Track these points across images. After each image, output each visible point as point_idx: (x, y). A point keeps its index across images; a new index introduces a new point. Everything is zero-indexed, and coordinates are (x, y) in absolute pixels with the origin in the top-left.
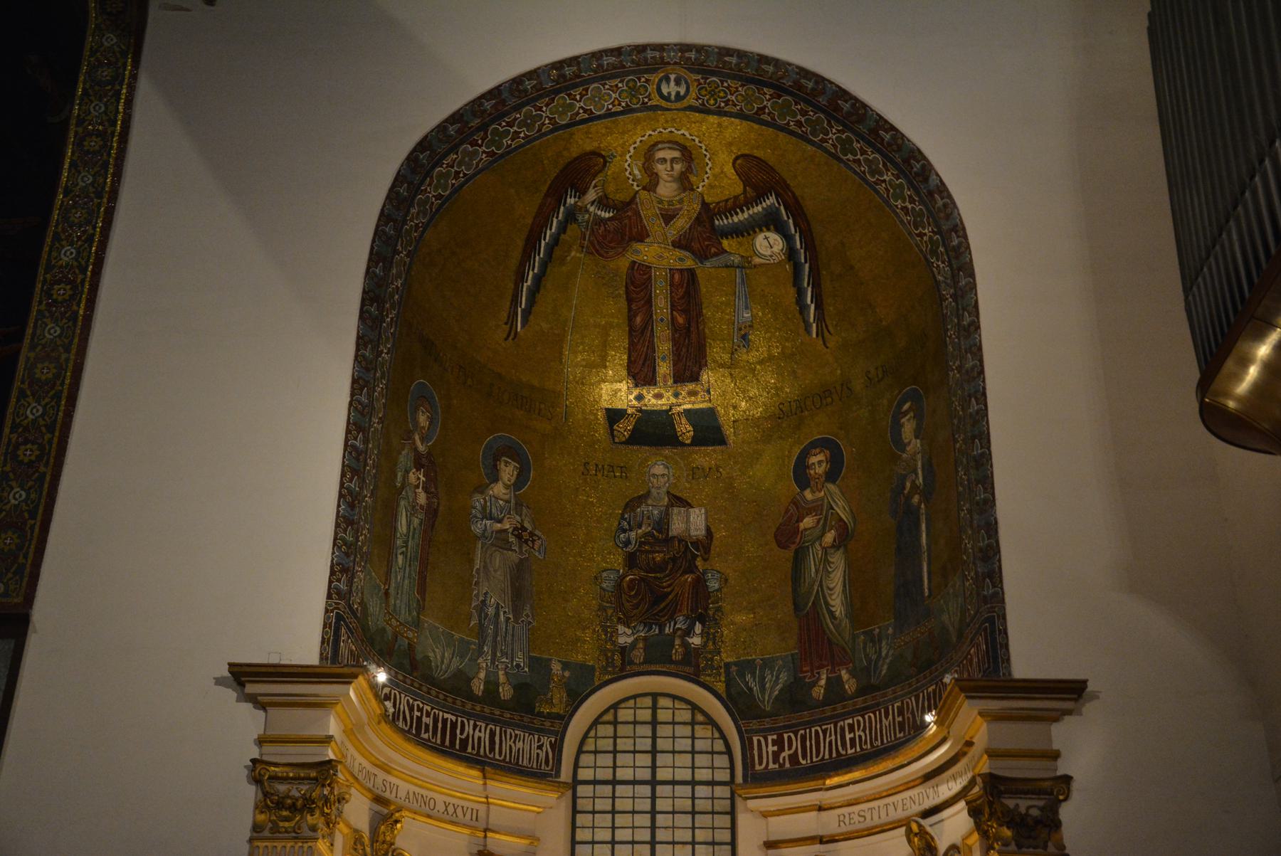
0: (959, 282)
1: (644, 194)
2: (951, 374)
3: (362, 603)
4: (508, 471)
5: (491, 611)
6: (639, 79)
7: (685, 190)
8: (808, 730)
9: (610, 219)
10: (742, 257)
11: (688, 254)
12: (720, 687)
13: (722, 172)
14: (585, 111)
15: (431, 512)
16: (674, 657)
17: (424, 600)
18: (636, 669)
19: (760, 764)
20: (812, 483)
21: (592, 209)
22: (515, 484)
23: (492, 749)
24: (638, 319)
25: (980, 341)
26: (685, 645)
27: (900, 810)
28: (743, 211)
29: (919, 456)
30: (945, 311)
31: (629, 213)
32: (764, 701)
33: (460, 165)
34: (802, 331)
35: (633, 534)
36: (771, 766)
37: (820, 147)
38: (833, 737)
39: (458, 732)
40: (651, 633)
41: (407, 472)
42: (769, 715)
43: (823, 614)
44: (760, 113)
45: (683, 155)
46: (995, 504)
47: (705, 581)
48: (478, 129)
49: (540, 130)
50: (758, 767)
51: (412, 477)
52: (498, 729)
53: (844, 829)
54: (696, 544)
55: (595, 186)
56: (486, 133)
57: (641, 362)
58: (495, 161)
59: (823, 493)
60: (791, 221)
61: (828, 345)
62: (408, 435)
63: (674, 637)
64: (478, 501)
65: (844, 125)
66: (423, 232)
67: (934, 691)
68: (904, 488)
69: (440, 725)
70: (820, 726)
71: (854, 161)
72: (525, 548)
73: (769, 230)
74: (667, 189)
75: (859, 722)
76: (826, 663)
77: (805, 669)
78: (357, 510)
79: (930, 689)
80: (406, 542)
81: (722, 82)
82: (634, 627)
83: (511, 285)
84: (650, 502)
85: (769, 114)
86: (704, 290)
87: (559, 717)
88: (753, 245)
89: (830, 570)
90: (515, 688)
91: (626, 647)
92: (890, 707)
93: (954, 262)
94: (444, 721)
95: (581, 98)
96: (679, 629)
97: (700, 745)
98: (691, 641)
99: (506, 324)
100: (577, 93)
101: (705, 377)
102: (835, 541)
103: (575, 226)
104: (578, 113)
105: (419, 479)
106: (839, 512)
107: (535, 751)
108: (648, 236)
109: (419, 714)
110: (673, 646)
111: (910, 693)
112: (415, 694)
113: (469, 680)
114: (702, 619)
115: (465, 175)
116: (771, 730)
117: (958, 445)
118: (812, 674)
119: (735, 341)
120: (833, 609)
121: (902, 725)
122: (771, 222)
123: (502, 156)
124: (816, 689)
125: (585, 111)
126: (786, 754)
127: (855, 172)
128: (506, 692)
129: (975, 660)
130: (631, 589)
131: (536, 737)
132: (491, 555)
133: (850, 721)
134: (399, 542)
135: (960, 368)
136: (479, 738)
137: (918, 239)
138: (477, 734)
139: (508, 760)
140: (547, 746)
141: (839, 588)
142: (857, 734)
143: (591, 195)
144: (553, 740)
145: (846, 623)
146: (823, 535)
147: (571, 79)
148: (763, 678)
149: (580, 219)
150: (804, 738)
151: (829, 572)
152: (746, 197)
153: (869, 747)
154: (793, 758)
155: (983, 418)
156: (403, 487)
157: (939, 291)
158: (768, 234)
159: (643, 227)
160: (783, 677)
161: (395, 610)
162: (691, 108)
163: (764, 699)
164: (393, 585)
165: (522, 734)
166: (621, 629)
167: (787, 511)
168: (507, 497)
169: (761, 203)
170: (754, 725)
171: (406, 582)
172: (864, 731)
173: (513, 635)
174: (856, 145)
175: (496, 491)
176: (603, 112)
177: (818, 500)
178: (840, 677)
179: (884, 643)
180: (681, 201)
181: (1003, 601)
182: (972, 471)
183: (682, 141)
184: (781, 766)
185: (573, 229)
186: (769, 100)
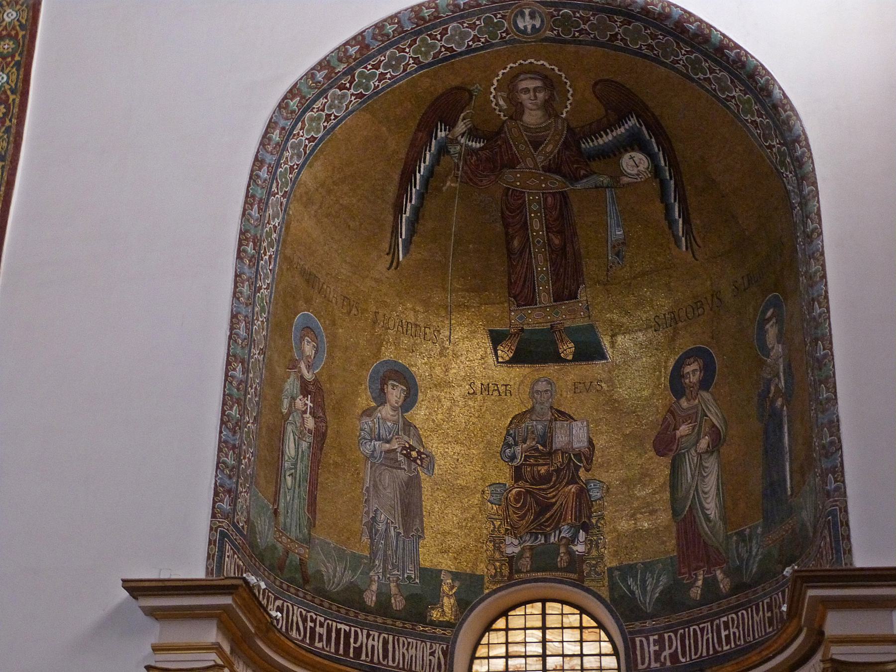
3: (248, 521)
6: (495, 16)
12: (605, 593)
15: (320, 436)
16: (559, 564)
23: (385, 656)
25: (823, 247)
26: (570, 553)
28: (607, 134)
32: (645, 603)
39: (352, 640)
42: (651, 617)
43: (699, 517)
47: (588, 491)
51: (299, 403)
52: (391, 638)
54: (578, 456)
60: (653, 140)
63: (559, 546)
69: (334, 635)
73: (633, 150)
74: (532, 117)
77: (683, 571)
80: (295, 465)
81: (574, 13)
82: (521, 538)
88: (619, 165)
89: (705, 474)
91: (513, 556)
94: (338, 631)
95: (441, 38)
98: (575, 548)
102: (708, 446)
105: (306, 404)
106: (712, 418)
107: (427, 658)
110: (559, 554)
112: (307, 605)
113: (361, 592)
114: (586, 527)
118: (690, 574)
120: (708, 512)
122: (634, 142)
132: (381, 474)
136: (373, 646)
139: (401, 666)
141: (713, 492)
146: (697, 441)
147: (430, 20)
148: (644, 581)
151: (704, 477)
155: (825, 320)
156: (290, 413)
158: (633, 154)
160: (664, 580)
163: (645, 601)
166: (509, 539)
170: (638, 625)
173: (404, 549)
177: (692, 408)
178: (715, 577)
179: (754, 542)
181: (845, 494)
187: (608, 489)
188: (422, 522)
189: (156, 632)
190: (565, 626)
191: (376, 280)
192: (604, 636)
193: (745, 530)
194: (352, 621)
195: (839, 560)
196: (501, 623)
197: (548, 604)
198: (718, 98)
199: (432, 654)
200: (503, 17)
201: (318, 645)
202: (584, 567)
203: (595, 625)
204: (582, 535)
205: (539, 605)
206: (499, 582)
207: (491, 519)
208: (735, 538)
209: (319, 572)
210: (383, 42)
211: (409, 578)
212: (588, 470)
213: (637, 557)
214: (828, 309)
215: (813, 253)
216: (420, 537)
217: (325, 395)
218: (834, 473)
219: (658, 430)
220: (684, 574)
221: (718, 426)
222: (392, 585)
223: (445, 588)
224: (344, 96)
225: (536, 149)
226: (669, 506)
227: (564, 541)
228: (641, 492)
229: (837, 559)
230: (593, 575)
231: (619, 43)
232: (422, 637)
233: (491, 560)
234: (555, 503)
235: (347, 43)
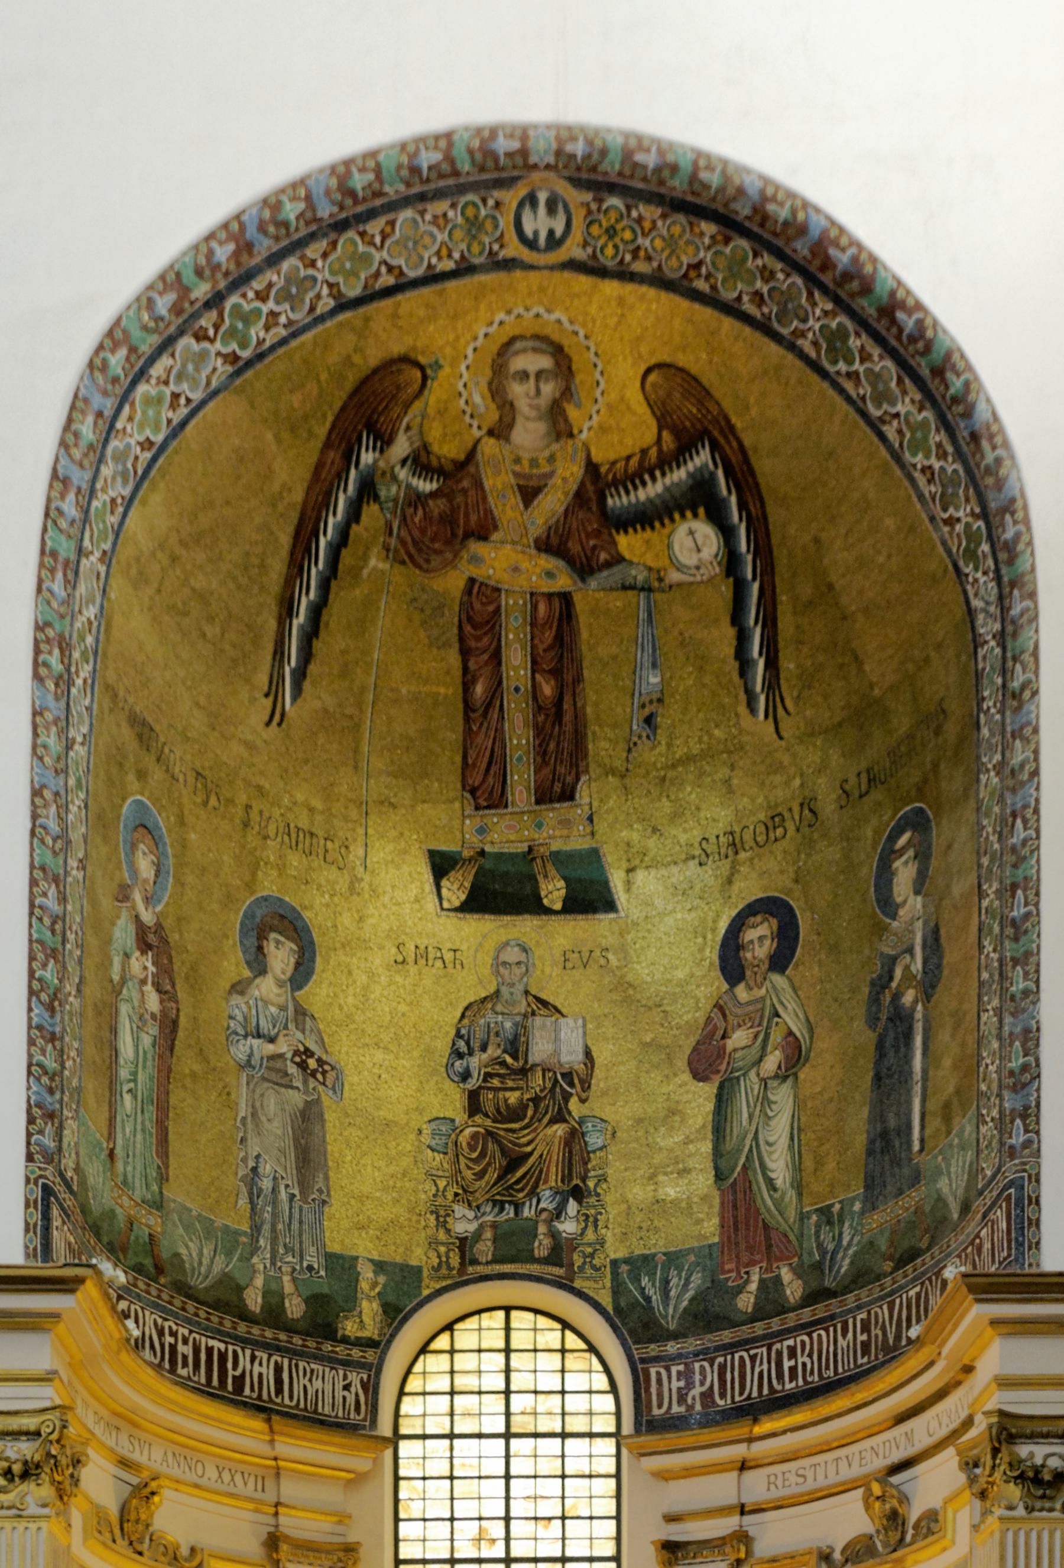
0: (1009, 608)
1: (490, 447)
2: (983, 778)
6: (484, 201)
7: (558, 437)
8: (729, 1357)
10: (650, 569)
11: (561, 564)
12: (606, 1299)
13: (622, 399)
14: (390, 269)
16: (536, 1252)
17: (167, 1167)
18: (481, 1269)
19: (660, 1406)
20: (748, 973)
22: (291, 980)
26: (554, 1235)
27: (855, 1464)
29: (919, 924)
30: (980, 666)
32: (666, 1316)
33: (180, 377)
34: (742, 709)
35: (474, 1062)
36: (676, 1409)
37: (792, 347)
38: (765, 1367)
40: (503, 1217)
41: (127, 956)
42: (675, 1336)
43: (757, 1183)
44: (692, 274)
45: (557, 364)
46: (1039, 1000)
47: (583, 1134)
48: (208, 305)
50: (656, 1412)
53: (775, 1494)
54: (568, 1076)
57: (484, 766)
58: (238, 373)
59: (763, 991)
61: (784, 734)
62: (123, 895)
63: (537, 1222)
64: (238, 1005)
66: (125, 515)
67: (918, 1295)
68: (891, 979)
70: (747, 1351)
71: (848, 375)
72: (312, 1083)
75: (803, 1343)
76: (757, 1257)
77: (727, 1267)
79: (912, 1293)
81: (628, 208)
82: (478, 1207)
83: (272, 624)
84: (499, 1008)
86: (584, 634)
87: (372, 1344)
89: (770, 1114)
90: (307, 1301)
91: (466, 1238)
92: (851, 1321)
93: (1004, 570)
95: (383, 242)
96: (544, 1210)
97: (573, 1382)
98: (561, 1227)
99: (267, 695)
101: (585, 793)
102: (779, 1067)
103: (375, 507)
105: (145, 968)
106: (788, 1020)
108: (496, 528)
109: (172, 1340)
110: (536, 1236)
111: (882, 1298)
114: (578, 1193)
116: (678, 1357)
117: (985, 903)
118: (739, 1273)
119: (635, 727)
120: (773, 1175)
121: (866, 1347)
124: (743, 1296)
126: (697, 1391)
128: (295, 1308)
129: (987, 1246)
130: (472, 1148)
131: (341, 1373)
132: (262, 1095)
133: (791, 1342)
134: (124, 1073)
135: (999, 768)
137: (946, 529)
138: (257, 1369)
140: (356, 1387)
141: (784, 1142)
142: (800, 1360)
144: (365, 1377)
145: (791, 1194)
146: (760, 1060)
147: (364, 200)
148: (666, 1282)
150: (722, 1368)
151: (769, 1118)
152: (660, 451)
153: (816, 1378)
154: (707, 1396)
157: (973, 629)
159: (489, 512)
160: (697, 1280)
161: (125, 1182)
162: (573, 265)
163: (666, 1311)
164: (120, 1142)
165: (321, 1368)
166: (460, 1210)
167: (709, 1019)
168: (281, 1000)
169: (685, 462)
170: (653, 1349)
171: (139, 1137)
172: (810, 1356)
173: (301, 1222)
175: (264, 989)
177: (756, 1001)
178: (778, 1279)
179: (847, 1225)
180: (552, 459)
182: (1007, 944)
183: (555, 337)
184: (690, 1408)
186: (709, 248)
187: (614, 1133)
188: (327, 1178)
190: (539, 1347)
192: (596, 1365)
193: (832, 1205)
196: (442, 1342)
197: (514, 1314)
198: (864, 414)
200: (498, 205)
202: (575, 1256)
203: (584, 1346)
204: (572, 1206)
205: (501, 1314)
206: (445, 1278)
207: (433, 1177)
208: (814, 1218)
210: (277, 239)
212: (583, 1101)
213: (657, 1245)
216: (324, 1202)
217: (173, 953)
218: (1024, 1116)
219: (697, 1037)
220: (730, 1271)
221: (798, 1034)
223: (364, 1285)
224: (203, 355)
226: (710, 1165)
227: (544, 1215)
228: (667, 1140)
230: (589, 1271)
231: (702, 285)
233: (433, 1243)
234: (531, 1154)
235: (211, 236)
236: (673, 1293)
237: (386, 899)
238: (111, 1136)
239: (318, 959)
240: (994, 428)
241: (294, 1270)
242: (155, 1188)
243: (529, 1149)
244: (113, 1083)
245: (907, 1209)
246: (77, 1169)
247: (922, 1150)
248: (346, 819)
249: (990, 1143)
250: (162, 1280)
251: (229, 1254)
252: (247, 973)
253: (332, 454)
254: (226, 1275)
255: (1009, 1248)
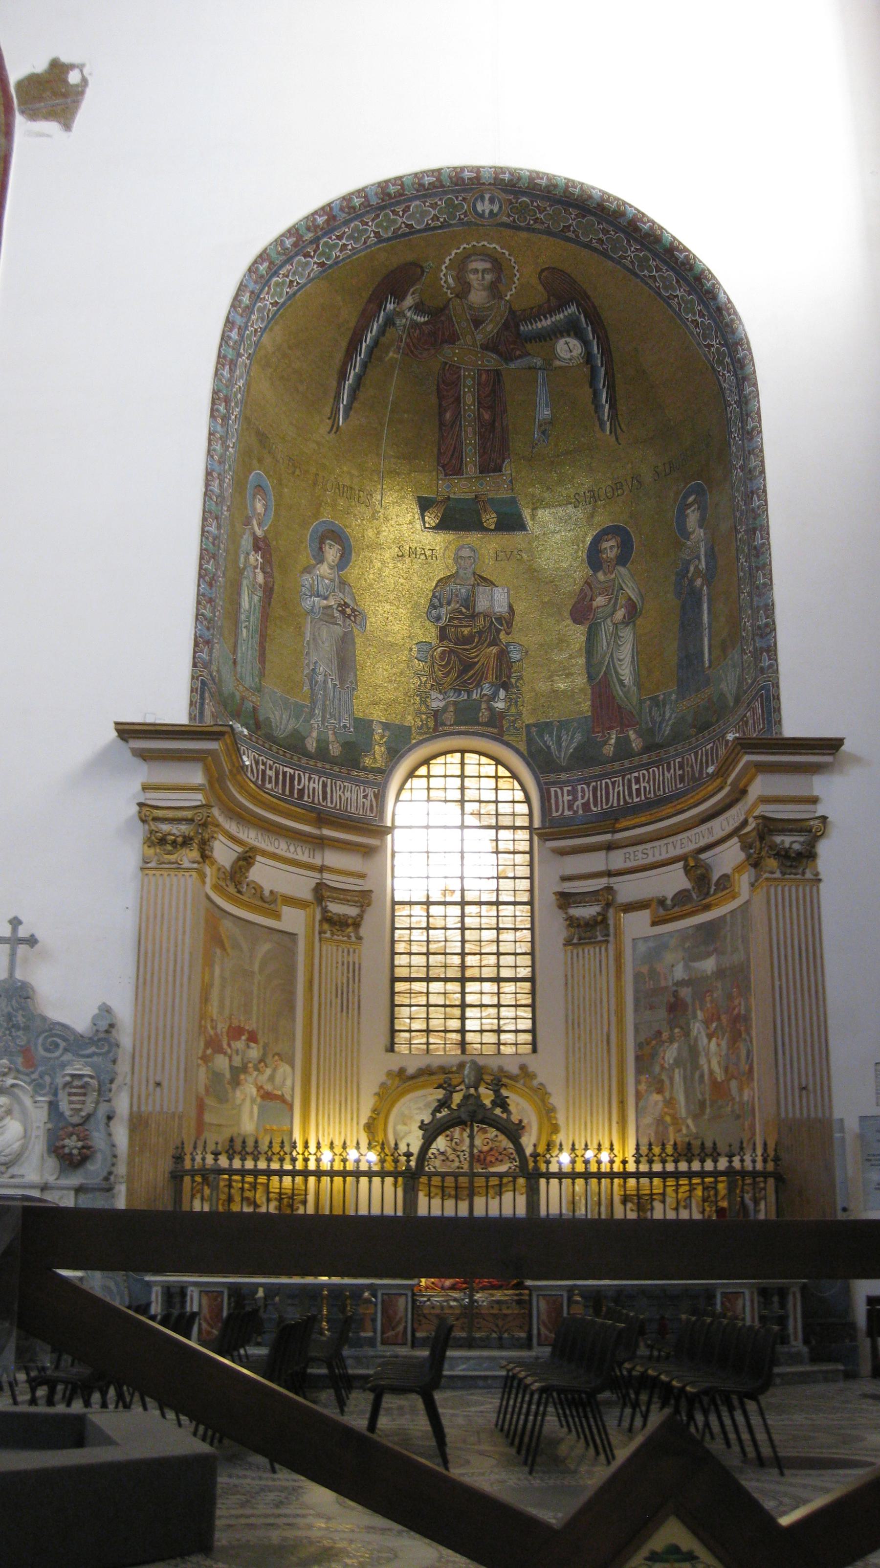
0: (743, 390)
4: (332, 553)
5: (320, 678)
9: (425, 323)
15: (268, 591)
21: (409, 314)
23: (325, 798)
24: (448, 415)
25: (762, 444)
26: (491, 709)
28: (546, 318)
29: (702, 544)
31: (443, 318)
35: (443, 611)
39: (296, 783)
47: (509, 653)
49: (365, 242)
51: (252, 558)
52: (329, 780)
54: (499, 619)
55: (413, 293)
56: (318, 247)
59: (613, 576)
60: (589, 328)
62: (247, 522)
64: (307, 579)
65: (642, 244)
68: (688, 572)
69: (281, 777)
72: (348, 621)
73: (569, 335)
74: (478, 297)
76: (615, 725)
77: (596, 730)
78: (214, 589)
80: (248, 617)
82: (445, 693)
85: (574, 232)
88: (554, 349)
94: (285, 773)
96: (485, 695)
97: (503, 795)
98: (495, 705)
100: (399, 209)
102: (624, 617)
104: (400, 227)
105: (257, 560)
106: (628, 591)
107: (361, 800)
110: (480, 709)
112: (258, 749)
113: (304, 738)
114: (506, 686)
115: (298, 284)
120: (623, 678)
122: (572, 329)
123: (331, 266)
124: (607, 747)
125: (407, 226)
127: (650, 287)
130: (442, 659)
132: (319, 629)
136: (314, 789)
139: (338, 807)
141: (628, 660)
143: (409, 301)
145: (634, 689)
148: (559, 738)
149: (398, 322)
151: (620, 646)
155: (763, 512)
157: (724, 397)
158: (568, 340)
160: (578, 737)
166: (434, 694)
167: (582, 590)
173: (340, 700)
174: (652, 263)
175: (322, 571)
176: (423, 226)
181: (777, 671)
185: (390, 332)
186: (574, 219)
187: (527, 652)
188: (356, 675)
189: (143, 773)
190: (482, 774)
191: (318, 443)
192: (517, 785)
194: (295, 765)
195: (770, 729)
196: (423, 771)
197: (467, 755)
199: (365, 797)
201: (268, 786)
202: (504, 722)
203: (509, 774)
204: (502, 693)
205: (458, 755)
206: (425, 733)
207: (418, 675)
209: (268, 718)
211: (345, 726)
213: (553, 716)
214: (766, 501)
215: (753, 450)
216: (354, 689)
217: (273, 552)
221: (635, 600)
222: (330, 732)
223: (377, 737)
225: (476, 327)
226: (584, 671)
227: (485, 698)
228: (559, 657)
229: (768, 730)
230: (513, 731)
232: (358, 782)
233: (418, 713)
236: (563, 744)
237: (393, 522)
238: (235, 652)
239: (353, 554)
240: (730, 306)
241: (335, 727)
242: (257, 680)
243: (476, 660)
244: (236, 623)
245: (703, 699)
246: (218, 671)
247: (710, 667)
248: (371, 480)
249: (749, 665)
250: (259, 733)
251: (297, 718)
252: (313, 562)
253: (371, 306)
254: (295, 730)
255: (764, 723)
